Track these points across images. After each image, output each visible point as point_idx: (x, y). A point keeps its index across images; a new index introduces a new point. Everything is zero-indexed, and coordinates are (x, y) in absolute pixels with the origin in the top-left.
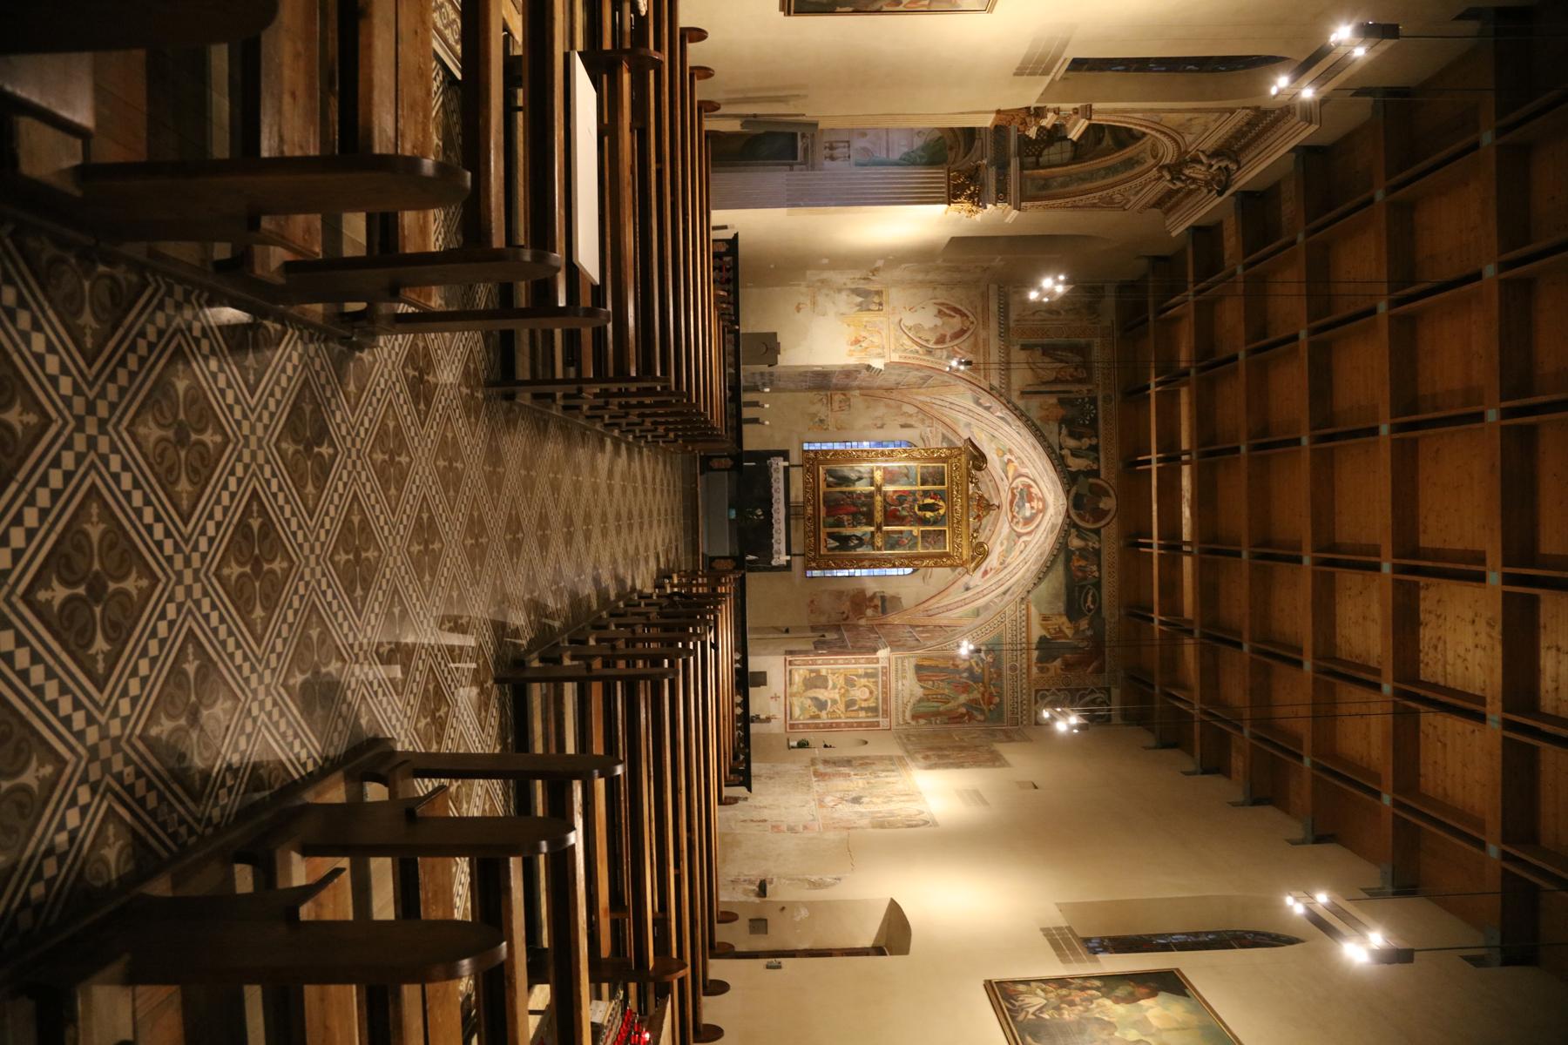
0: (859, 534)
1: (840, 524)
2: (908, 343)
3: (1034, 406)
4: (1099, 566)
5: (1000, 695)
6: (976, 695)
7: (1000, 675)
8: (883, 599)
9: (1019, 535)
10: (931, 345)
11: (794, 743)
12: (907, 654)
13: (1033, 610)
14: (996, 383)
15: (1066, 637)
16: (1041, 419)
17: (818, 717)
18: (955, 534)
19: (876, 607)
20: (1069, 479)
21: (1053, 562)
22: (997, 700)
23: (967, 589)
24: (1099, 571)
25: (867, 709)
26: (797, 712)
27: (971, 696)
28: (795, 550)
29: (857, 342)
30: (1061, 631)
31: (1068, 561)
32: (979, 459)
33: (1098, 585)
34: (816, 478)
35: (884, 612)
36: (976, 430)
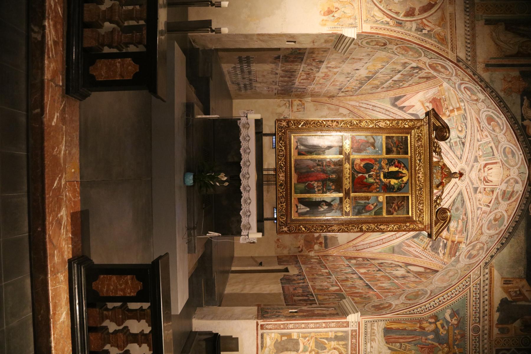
0: (328, 200)
1: (310, 190)
2: (379, 15)
3: (498, 79)
7: (463, 336)
8: (326, 238)
10: (401, 17)
12: (375, 318)
13: (496, 273)
14: (462, 55)
16: (504, 90)
18: (419, 201)
19: (321, 243)
21: (515, 228)
28: (267, 214)
29: (330, 12)
32: (442, 132)
34: (287, 146)
35: (326, 247)
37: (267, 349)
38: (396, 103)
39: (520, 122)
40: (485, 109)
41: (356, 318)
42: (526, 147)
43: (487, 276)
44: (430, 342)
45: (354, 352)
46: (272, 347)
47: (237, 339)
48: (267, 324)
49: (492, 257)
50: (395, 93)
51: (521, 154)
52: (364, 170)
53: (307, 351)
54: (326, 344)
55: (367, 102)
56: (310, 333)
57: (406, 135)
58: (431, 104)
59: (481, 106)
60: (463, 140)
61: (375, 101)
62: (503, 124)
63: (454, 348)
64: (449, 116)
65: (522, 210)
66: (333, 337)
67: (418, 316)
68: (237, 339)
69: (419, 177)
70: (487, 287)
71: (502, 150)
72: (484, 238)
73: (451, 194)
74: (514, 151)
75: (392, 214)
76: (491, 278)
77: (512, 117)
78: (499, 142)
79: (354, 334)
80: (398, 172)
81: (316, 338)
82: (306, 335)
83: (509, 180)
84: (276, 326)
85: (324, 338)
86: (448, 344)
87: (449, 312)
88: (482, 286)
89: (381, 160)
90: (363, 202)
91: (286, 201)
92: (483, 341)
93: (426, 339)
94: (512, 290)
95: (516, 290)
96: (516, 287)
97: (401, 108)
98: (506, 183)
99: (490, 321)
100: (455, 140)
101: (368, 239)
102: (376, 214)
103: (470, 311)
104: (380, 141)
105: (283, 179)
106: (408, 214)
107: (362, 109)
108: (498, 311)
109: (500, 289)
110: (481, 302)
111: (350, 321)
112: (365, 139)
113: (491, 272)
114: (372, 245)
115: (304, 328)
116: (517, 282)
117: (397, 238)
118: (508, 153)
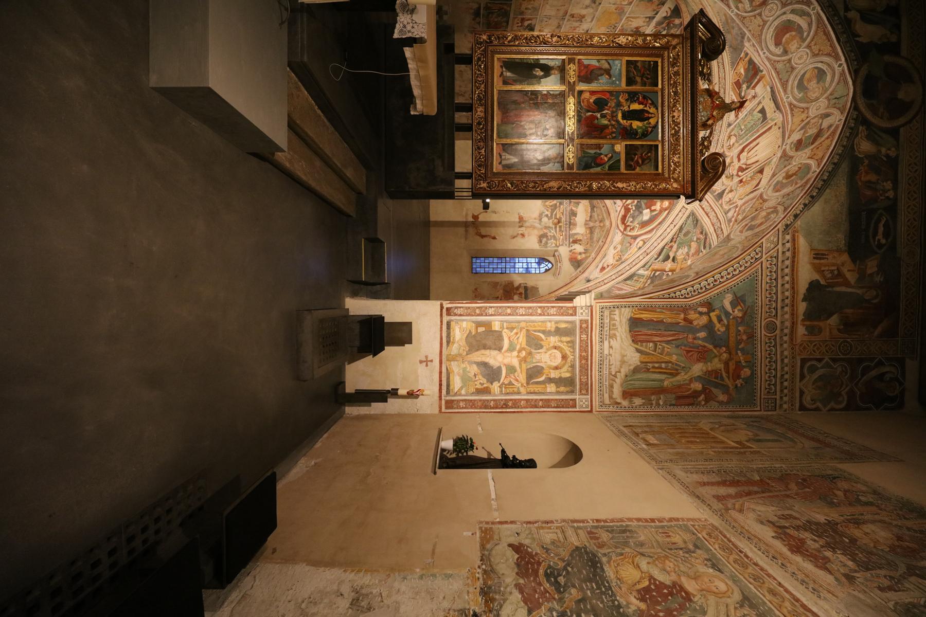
4: (895, 183)
5: (751, 365)
6: (717, 364)
7: (751, 336)
8: (526, 288)
11: (448, 444)
13: (802, 242)
15: (847, 284)
17: (486, 391)
19: (520, 294)
20: (859, 55)
21: (832, 174)
22: (746, 372)
23: (588, 281)
24: (895, 188)
25: (559, 382)
26: (457, 383)
27: (710, 367)
30: (840, 274)
31: (854, 171)
33: (892, 209)
37: (456, 345)
39: (842, 13)
40: (778, 13)
41: (588, 300)
42: (851, 51)
43: (788, 245)
44: (700, 342)
45: (584, 354)
46: (463, 343)
47: (409, 324)
48: (456, 308)
49: (796, 216)
51: (840, 65)
52: (595, 107)
53: (514, 349)
54: (542, 340)
56: (519, 322)
57: (656, 59)
59: (770, 11)
62: (810, 25)
63: (737, 354)
65: (843, 146)
66: (553, 329)
67: (682, 302)
68: (409, 324)
69: (673, 117)
70: (788, 263)
71: (796, 83)
74: (824, 67)
75: (634, 170)
76: (795, 249)
77: (830, 6)
78: (793, 69)
79: (584, 326)
80: (642, 111)
81: (528, 330)
82: (514, 325)
83: (808, 123)
84: (469, 311)
85: (539, 331)
86: (727, 347)
87: (729, 298)
88: (780, 260)
89: (618, 93)
90: (592, 152)
91: (486, 147)
92: (781, 345)
93: (694, 339)
94: (827, 268)
95: (833, 268)
96: (833, 265)
99: (792, 314)
102: (610, 168)
103: (762, 298)
104: (619, 67)
105: (482, 114)
106: (657, 169)
108: (804, 300)
109: (808, 267)
110: (779, 285)
111: (578, 305)
112: (597, 64)
113: (794, 240)
115: (509, 315)
116: (834, 257)
118: (809, 80)
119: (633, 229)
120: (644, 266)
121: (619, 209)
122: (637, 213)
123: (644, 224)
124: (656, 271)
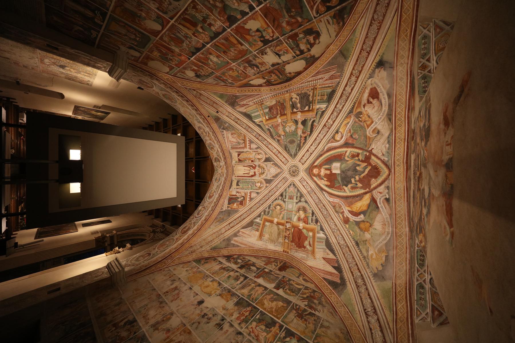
9: (346, 145)
23: (381, 64)
36: (376, 264)
38: (339, 281)
50: (331, 294)
55: (368, 333)
58: (305, 245)
60: (280, 198)
61: (359, 319)
64: (287, 222)
72: (207, 138)
73: (308, 154)
97: (338, 268)
98: (221, 166)
100: (291, 201)
101: (393, 27)
107: (389, 338)
114: (375, 26)
117: (351, 74)
119: (353, 156)
120: (323, 112)
121: (382, 188)
122: (350, 173)
123: (339, 158)
124: (309, 111)
